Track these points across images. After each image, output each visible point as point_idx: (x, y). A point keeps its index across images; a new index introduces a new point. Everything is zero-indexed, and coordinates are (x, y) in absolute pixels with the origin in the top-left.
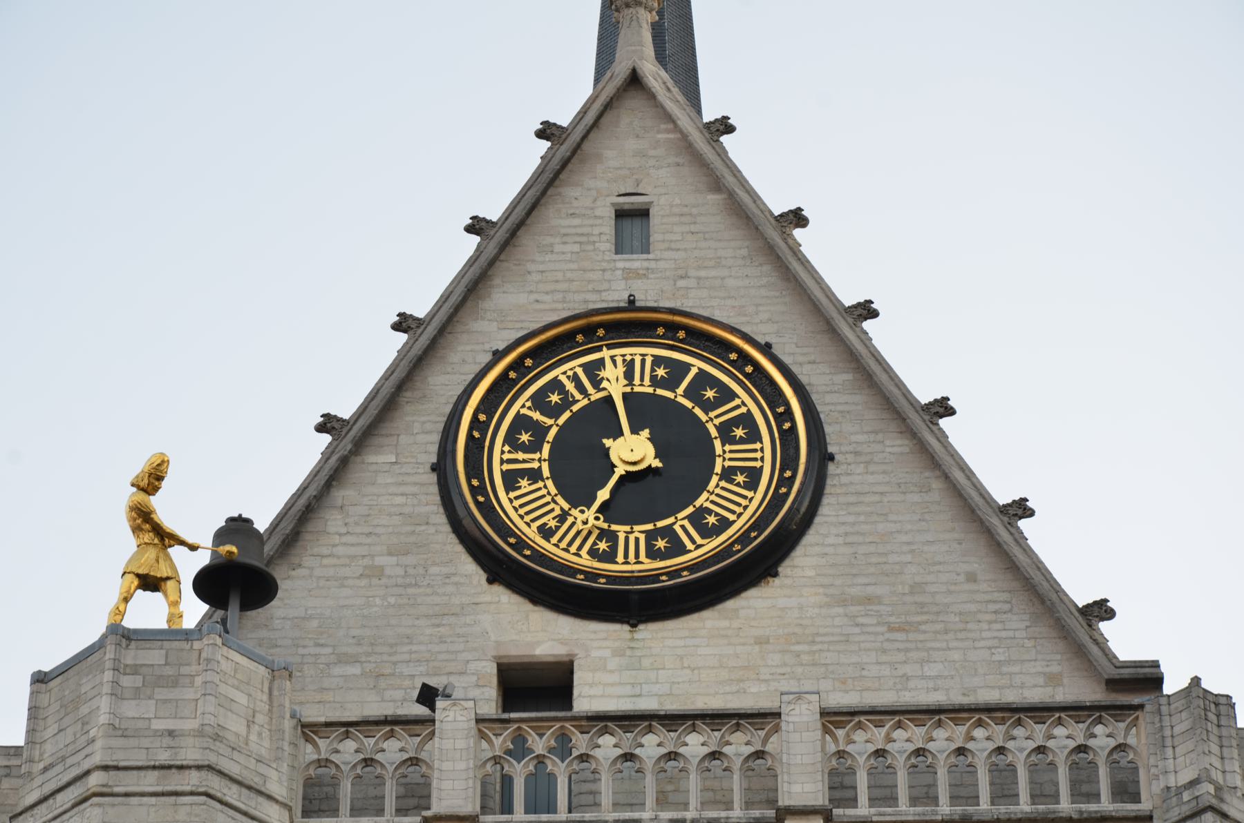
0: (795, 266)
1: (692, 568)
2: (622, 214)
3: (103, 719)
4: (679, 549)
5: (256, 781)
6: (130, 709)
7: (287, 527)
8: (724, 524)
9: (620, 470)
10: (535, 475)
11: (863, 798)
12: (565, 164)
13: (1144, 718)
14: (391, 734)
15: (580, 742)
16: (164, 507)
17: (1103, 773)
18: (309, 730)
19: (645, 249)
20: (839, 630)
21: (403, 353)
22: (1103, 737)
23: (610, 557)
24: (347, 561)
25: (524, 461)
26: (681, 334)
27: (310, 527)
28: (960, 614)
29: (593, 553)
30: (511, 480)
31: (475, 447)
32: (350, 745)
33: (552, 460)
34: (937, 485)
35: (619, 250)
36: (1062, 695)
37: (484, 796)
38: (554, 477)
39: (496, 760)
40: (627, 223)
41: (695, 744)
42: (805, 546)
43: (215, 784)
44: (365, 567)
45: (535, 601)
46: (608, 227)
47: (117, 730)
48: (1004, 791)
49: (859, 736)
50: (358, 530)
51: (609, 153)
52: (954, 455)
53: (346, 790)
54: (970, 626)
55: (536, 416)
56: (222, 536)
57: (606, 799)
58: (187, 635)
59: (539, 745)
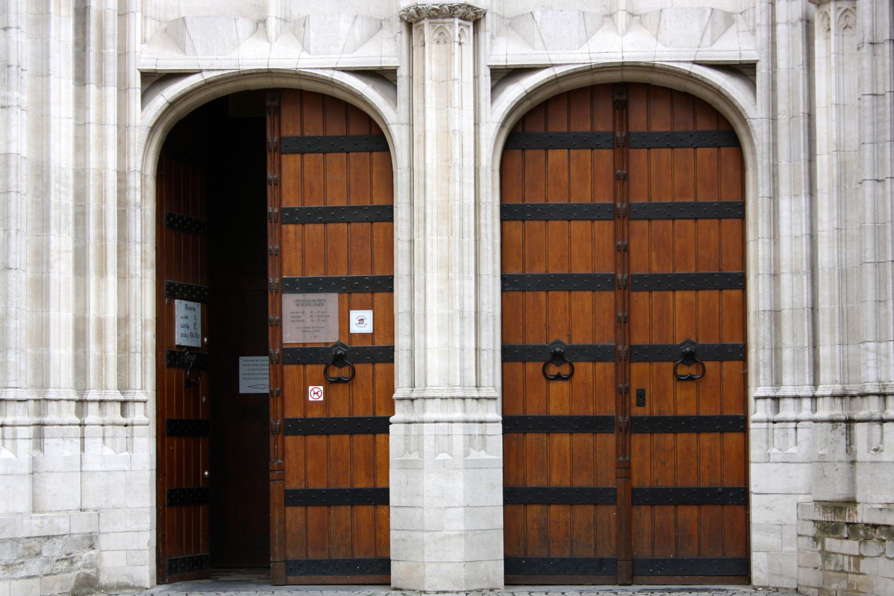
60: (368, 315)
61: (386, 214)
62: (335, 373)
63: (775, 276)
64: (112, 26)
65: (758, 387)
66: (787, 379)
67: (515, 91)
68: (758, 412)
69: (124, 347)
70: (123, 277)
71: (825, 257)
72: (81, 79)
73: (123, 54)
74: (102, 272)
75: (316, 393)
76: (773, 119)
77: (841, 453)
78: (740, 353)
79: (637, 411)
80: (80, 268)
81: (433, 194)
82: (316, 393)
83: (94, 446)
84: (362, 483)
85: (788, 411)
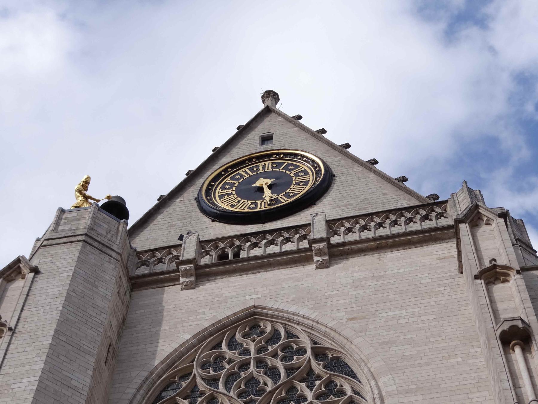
20: (337, 214)
24: (163, 224)
25: (226, 192)
26: (281, 155)
28: (381, 203)
42: (325, 196)
44: (169, 225)
50: (168, 217)
54: (385, 205)
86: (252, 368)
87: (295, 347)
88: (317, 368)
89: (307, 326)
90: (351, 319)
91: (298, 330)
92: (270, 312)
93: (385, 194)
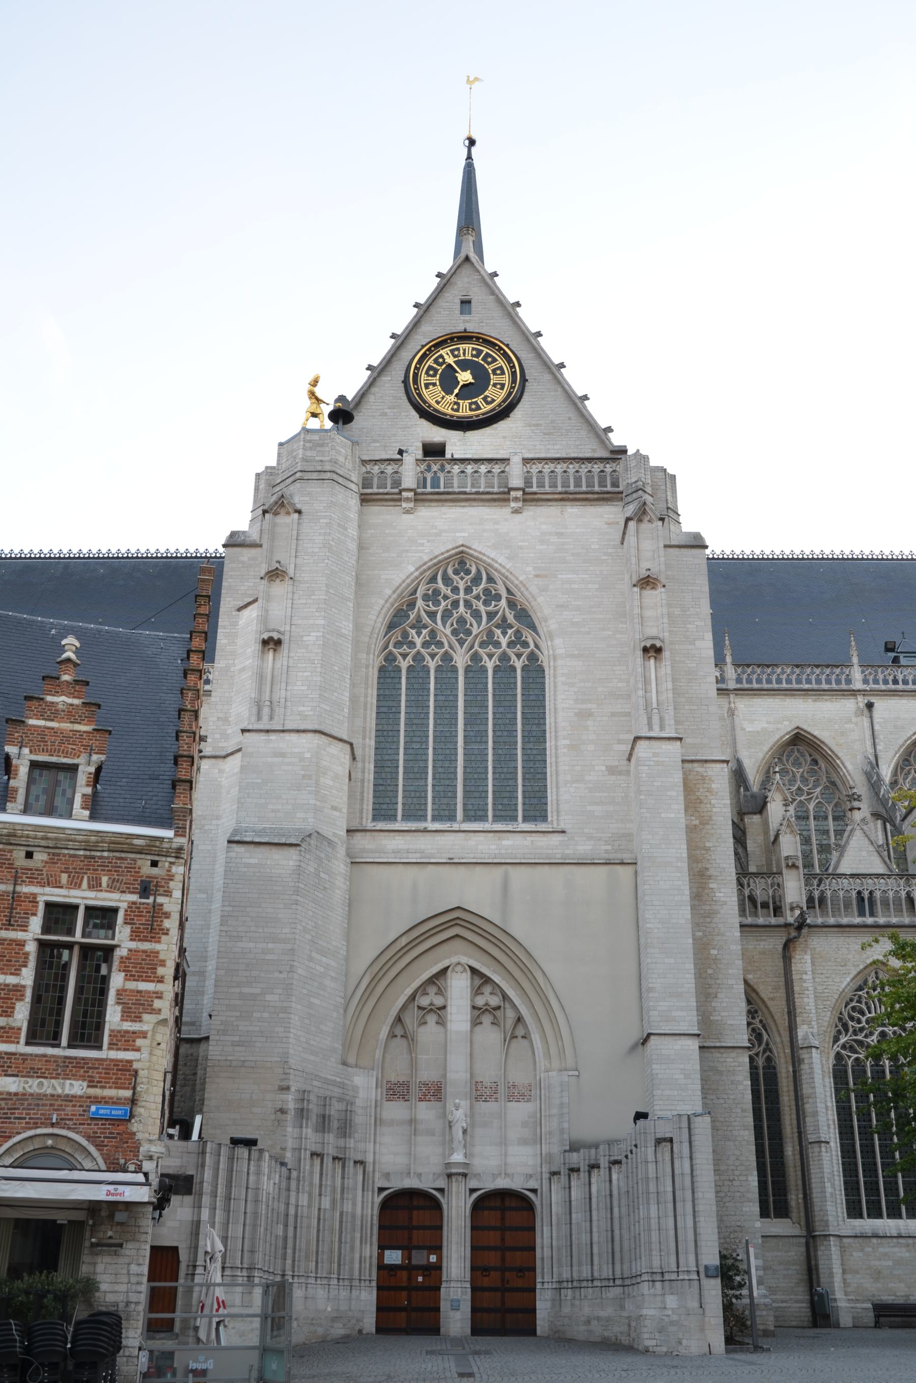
0: (517, 319)
1: (483, 414)
2: (463, 302)
3: (300, 456)
4: (478, 408)
5: (348, 476)
6: (309, 453)
7: (357, 399)
8: (493, 401)
9: (461, 383)
10: (434, 385)
11: (535, 485)
12: (445, 285)
13: (622, 462)
14: (389, 464)
15: (448, 467)
16: (319, 391)
17: (608, 479)
18: (364, 462)
19: (470, 313)
21: (393, 346)
22: (608, 468)
23: (457, 410)
27: (364, 400)
29: (452, 409)
30: (427, 386)
31: (416, 375)
32: (376, 467)
33: (440, 380)
34: (560, 389)
35: (461, 313)
36: (596, 455)
37: (418, 484)
38: (440, 385)
39: (422, 472)
40: (464, 305)
41: (483, 469)
43: (335, 477)
45: (434, 424)
46: (458, 306)
47: (305, 460)
48: (578, 483)
49: (534, 467)
51: (459, 282)
52: (565, 380)
53: (375, 480)
55: (435, 366)
56: (337, 401)
57: (456, 484)
58: (326, 431)
59: (435, 468)
60: (435, 1256)
61: (440, 1228)
62: (426, 1273)
63: (543, 1248)
64: (371, 1175)
65: (539, 1280)
66: (546, 1277)
67: (475, 1195)
68: (539, 1286)
69: (371, 1265)
70: (371, 1244)
71: (554, 1243)
72: (363, 1190)
73: (373, 1182)
74: (366, 1243)
75: (420, 1279)
76: (542, 1205)
77: (558, 1298)
78: (534, 1269)
79: (507, 1286)
80: (361, 1243)
81: (454, 1224)
82: (420, 1279)
83: (363, 1293)
84: (432, 1305)
85: (546, 1286)
86: (462, 608)
87: (494, 592)
88: (510, 618)
89: (503, 575)
90: (537, 576)
91: (496, 575)
92: (476, 554)
93: (570, 419)
